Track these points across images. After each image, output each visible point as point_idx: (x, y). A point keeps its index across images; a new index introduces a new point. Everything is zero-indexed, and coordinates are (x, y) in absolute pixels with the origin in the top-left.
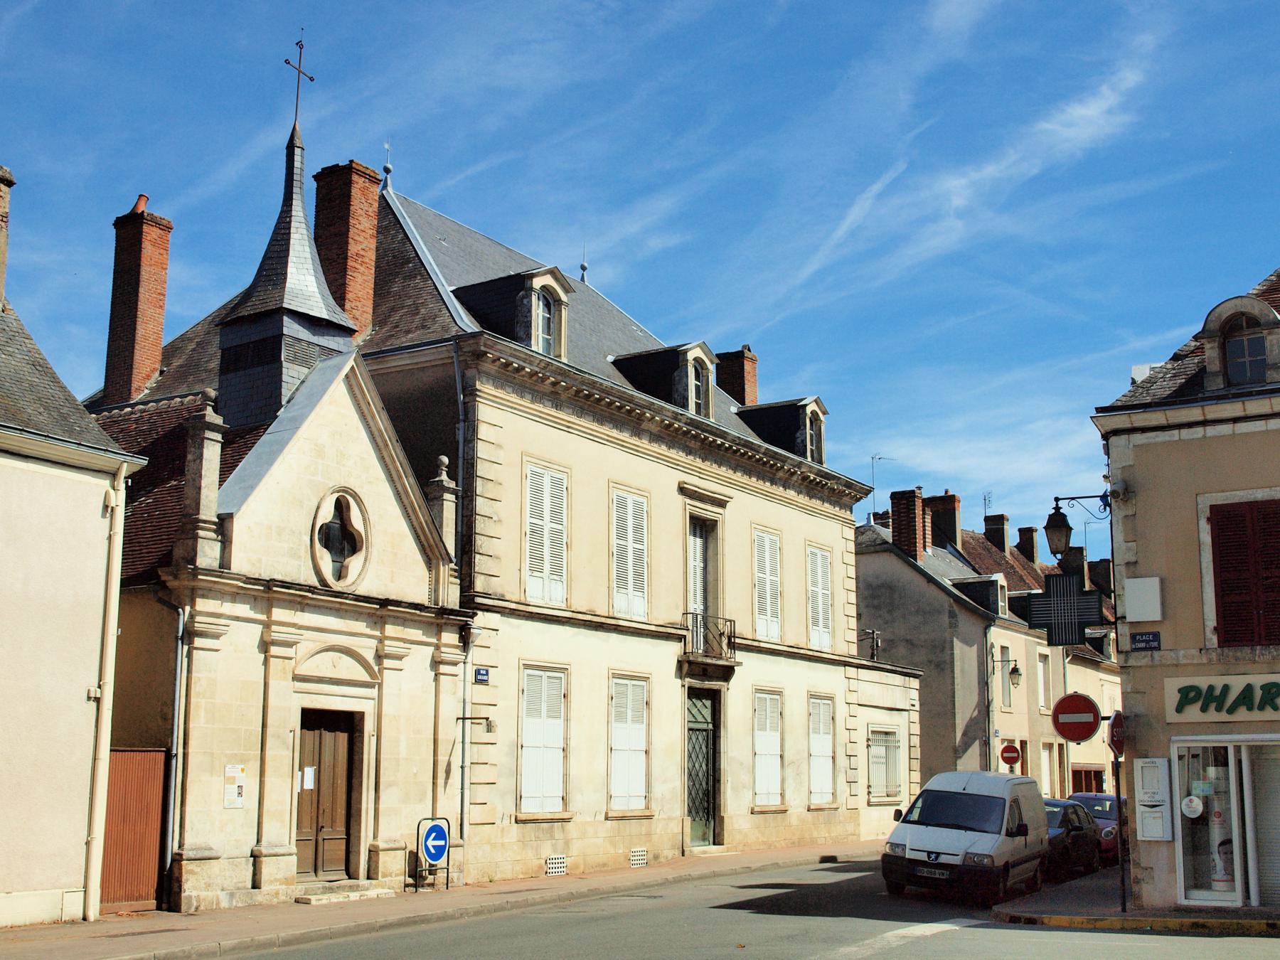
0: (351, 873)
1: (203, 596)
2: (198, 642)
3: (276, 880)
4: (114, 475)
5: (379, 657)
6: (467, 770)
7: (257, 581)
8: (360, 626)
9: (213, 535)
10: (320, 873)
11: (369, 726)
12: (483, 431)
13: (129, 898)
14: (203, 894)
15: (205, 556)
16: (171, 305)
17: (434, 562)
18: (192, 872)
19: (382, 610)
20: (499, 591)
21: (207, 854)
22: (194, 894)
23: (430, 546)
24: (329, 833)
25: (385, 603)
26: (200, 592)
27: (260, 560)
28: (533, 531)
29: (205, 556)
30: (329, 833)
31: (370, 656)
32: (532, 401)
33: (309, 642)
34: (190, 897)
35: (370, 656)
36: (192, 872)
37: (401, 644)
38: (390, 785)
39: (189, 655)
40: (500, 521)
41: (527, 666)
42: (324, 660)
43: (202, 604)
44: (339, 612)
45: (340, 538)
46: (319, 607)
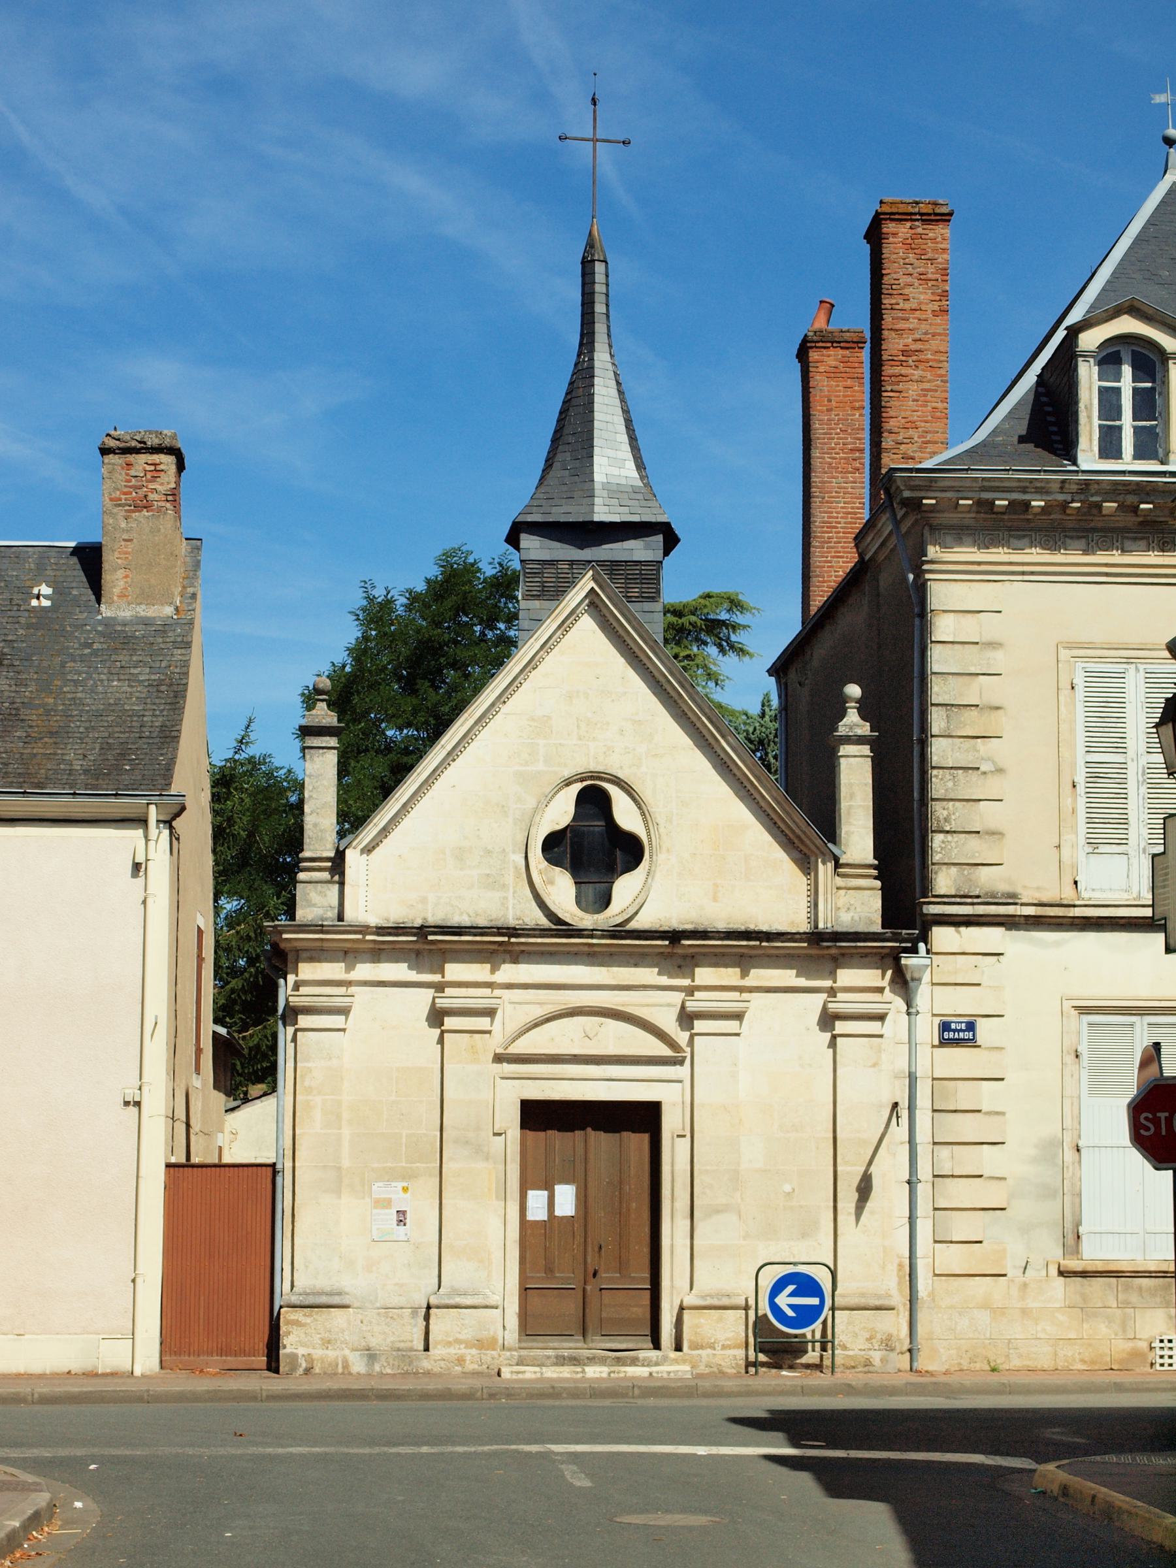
0: (657, 1345)
1: (311, 959)
2: (304, 1021)
3: (458, 1341)
4: (142, 822)
5: (687, 1018)
6: (923, 1190)
7: (398, 930)
8: (648, 975)
9: (326, 875)
10: (589, 1338)
11: (671, 1122)
12: (943, 627)
13: (223, 1351)
14: (318, 1353)
15: (311, 904)
16: (624, 472)
17: (813, 859)
18: (297, 1323)
19: (678, 948)
20: (1003, 887)
21: (336, 1300)
22: (301, 1351)
23: (798, 837)
24: (611, 1280)
25: (675, 936)
26: (304, 955)
27: (424, 900)
28: (1093, 777)
29: (311, 904)
30: (611, 1280)
31: (668, 1021)
32: (1086, 552)
33: (515, 1010)
34: (294, 1357)
35: (668, 1021)
36: (297, 1323)
37: (735, 995)
38: (717, 1210)
39: (294, 1040)
40: (1000, 771)
41: (1084, 1010)
42: (579, 1029)
43: (307, 971)
44: (592, 957)
45: (596, 844)
46: (551, 954)
